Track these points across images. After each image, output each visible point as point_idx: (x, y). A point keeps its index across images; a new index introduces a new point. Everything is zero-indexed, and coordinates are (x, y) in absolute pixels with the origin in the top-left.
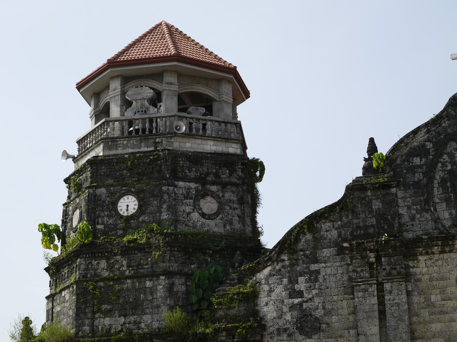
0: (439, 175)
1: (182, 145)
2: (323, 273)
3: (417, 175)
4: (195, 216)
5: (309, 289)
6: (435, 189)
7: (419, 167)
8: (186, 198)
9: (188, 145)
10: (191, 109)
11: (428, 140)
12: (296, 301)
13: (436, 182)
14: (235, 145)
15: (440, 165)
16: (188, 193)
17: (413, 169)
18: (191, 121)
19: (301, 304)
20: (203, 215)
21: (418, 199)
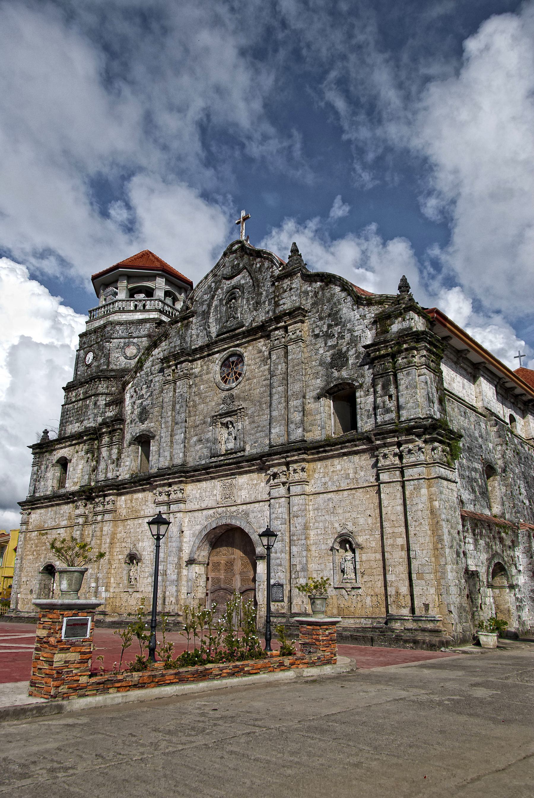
0: (215, 303)
1: (120, 317)
2: (154, 381)
3: (204, 307)
4: (122, 358)
5: (147, 392)
6: (211, 314)
7: (206, 300)
8: (117, 348)
9: (124, 317)
10: (135, 296)
11: (214, 282)
12: (140, 401)
13: (212, 308)
14: (154, 313)
15: (216, 296)
16: (119, 346)
17: (202, 304)
18: (136, 303)
19: (142, 403)
20: (126, 358)
21: (202, 322)
